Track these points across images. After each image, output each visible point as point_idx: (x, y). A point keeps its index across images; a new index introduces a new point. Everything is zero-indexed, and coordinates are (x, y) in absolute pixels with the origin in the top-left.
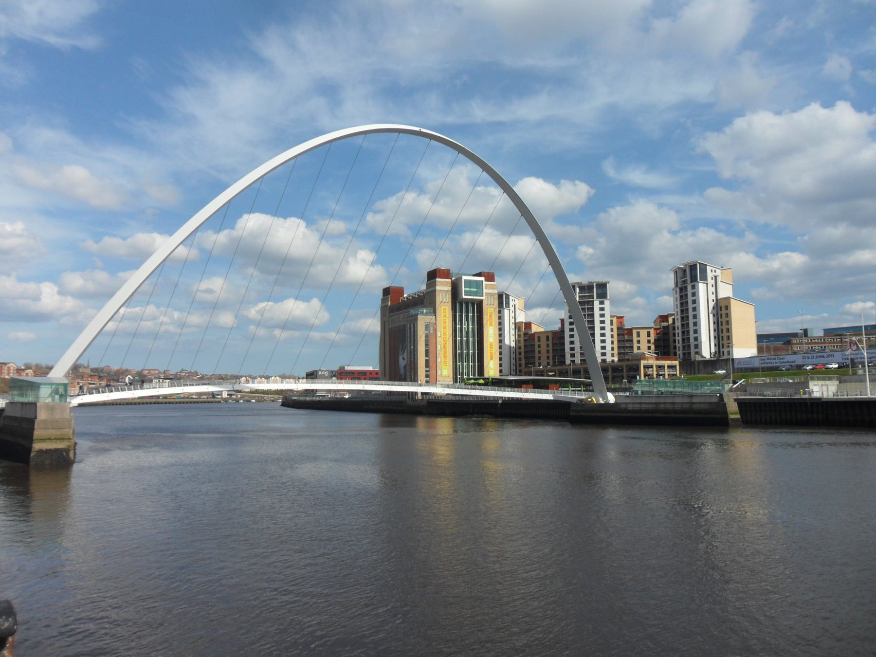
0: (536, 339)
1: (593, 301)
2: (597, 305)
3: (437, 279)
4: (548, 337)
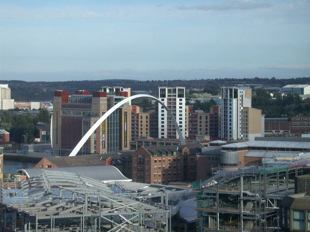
0: (140, 117)
1: (175, 99)
2: (178, 99)
3: (101, 98)
4: (147, 117)
